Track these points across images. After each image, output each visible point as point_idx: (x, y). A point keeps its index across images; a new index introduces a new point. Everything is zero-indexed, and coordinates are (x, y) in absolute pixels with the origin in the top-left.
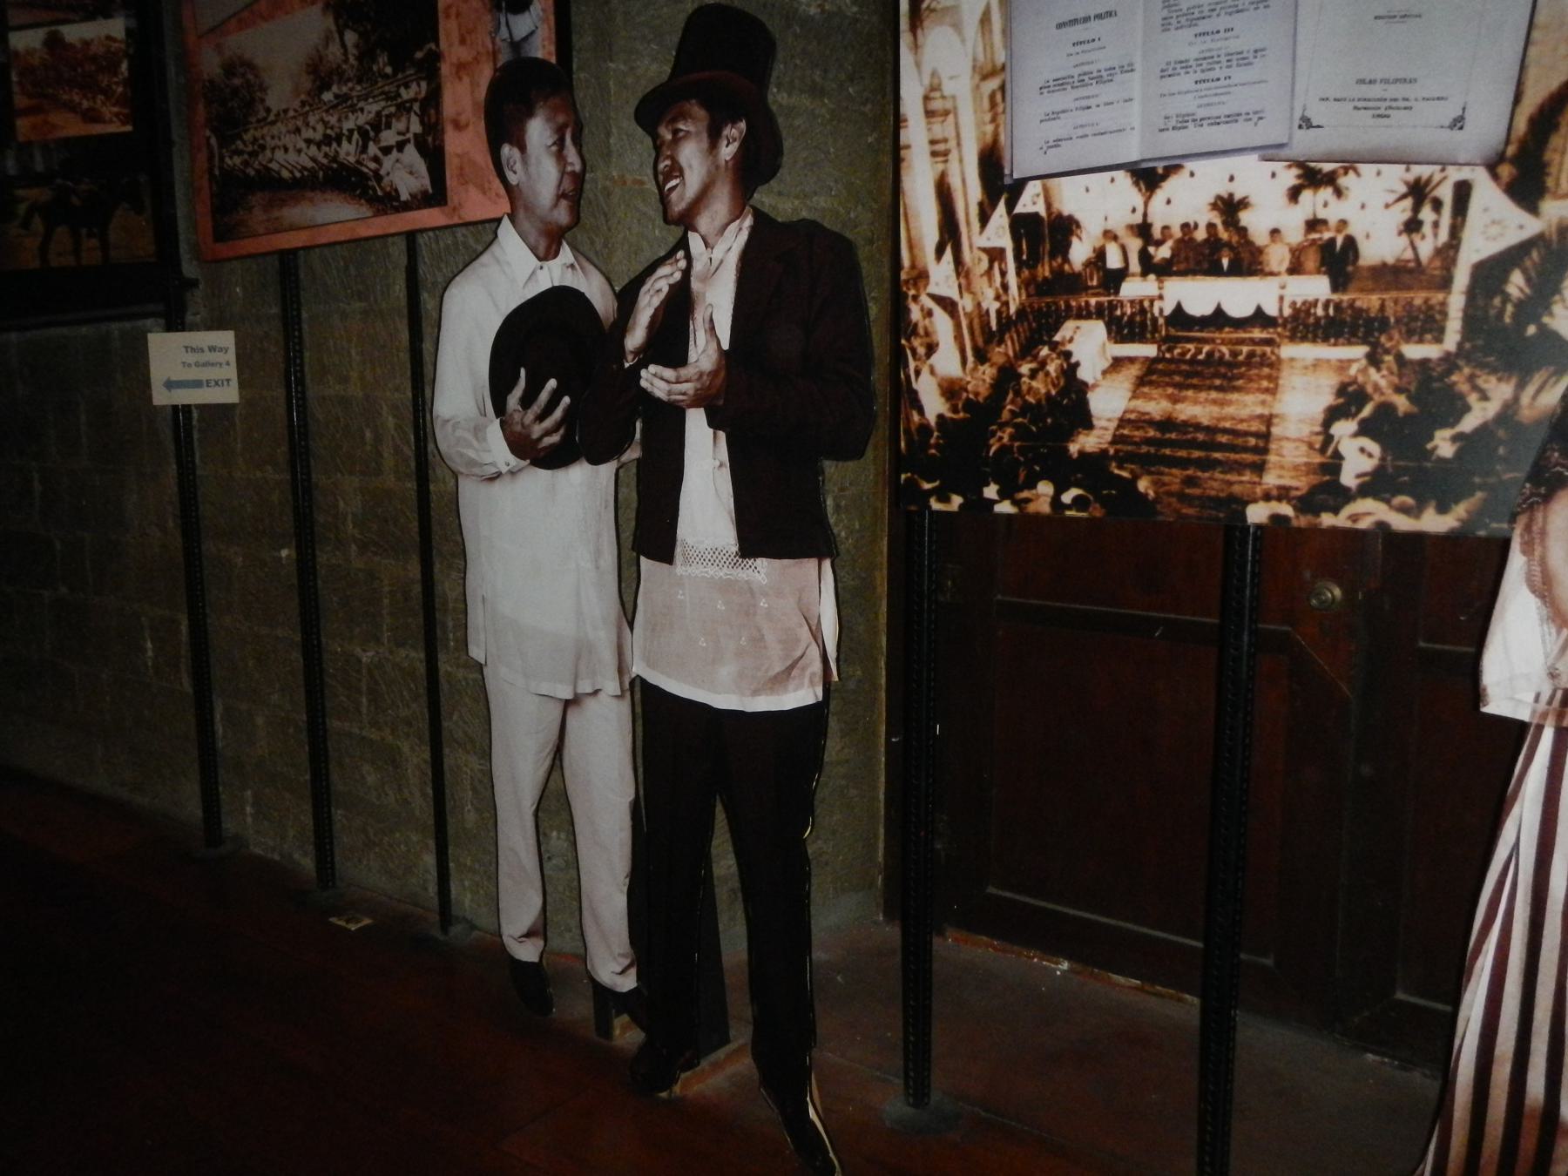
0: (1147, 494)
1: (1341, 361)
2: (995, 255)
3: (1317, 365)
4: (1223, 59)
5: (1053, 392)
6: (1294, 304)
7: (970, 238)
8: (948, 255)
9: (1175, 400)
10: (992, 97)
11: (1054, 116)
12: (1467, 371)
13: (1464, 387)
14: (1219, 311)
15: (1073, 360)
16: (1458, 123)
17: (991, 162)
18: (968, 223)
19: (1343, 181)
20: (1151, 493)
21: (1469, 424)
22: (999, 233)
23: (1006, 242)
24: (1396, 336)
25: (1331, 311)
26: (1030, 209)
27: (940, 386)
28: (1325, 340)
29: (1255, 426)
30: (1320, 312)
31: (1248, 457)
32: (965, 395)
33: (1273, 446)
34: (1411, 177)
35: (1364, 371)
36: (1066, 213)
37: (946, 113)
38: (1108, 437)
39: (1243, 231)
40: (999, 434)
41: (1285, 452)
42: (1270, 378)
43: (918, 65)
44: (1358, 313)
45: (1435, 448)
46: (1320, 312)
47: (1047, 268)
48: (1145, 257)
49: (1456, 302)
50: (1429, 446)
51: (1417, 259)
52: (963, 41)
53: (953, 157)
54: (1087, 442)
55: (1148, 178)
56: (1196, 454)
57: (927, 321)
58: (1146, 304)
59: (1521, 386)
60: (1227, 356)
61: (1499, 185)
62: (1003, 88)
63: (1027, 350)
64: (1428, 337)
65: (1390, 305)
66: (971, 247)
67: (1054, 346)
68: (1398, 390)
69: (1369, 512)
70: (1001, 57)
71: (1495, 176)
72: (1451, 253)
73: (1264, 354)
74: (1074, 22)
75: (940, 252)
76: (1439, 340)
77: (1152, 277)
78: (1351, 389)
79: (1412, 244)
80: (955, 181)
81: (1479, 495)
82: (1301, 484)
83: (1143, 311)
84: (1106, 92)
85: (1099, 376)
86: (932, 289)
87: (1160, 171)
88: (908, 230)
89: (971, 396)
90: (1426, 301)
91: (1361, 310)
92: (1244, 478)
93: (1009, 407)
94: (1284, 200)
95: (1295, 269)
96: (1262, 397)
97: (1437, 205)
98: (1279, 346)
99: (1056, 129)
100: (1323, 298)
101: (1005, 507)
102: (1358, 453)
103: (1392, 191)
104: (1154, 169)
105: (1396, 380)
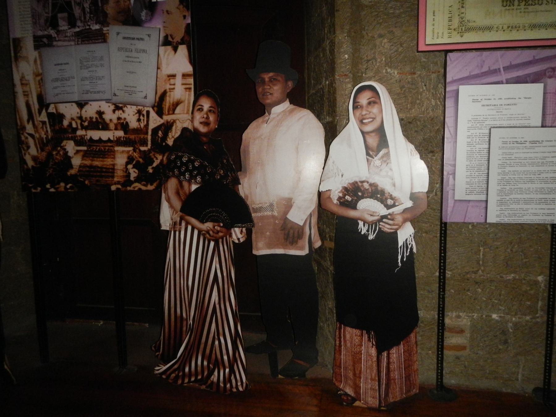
0: (88, 185)
1: (128, 151)
2: (44, 123)
3: (123, 152)
4: (95, 78)
5: (62, 159)
7: (36, 119)
8: (31, 122)
9: (92, 161)
10: (39, 81)
11: (55, 88)
12: (153, 153)
13: (153, 157)
14: (100, 139)
15: (67, 150)
16: (146, 97)
17: (41, 98)
18: (36, 114)
19: (125, 109)
20: (89, 184)
21: (155, 165)
22: (44, 117)
23: (46, 119)
24: (138, 145)
26: (52, 111)
27: (31, 158)
29: (111, 167)
30: (122, 139)
31: (110, 174)
32: (39, 160)
33: (115, 171)
34: (137, 109)
35: (133, 153)
36: (61, 113)
37: (27, 84)
38: (77, 170)
39: (104, 119)
40: (49, 170)
41: (118, 173)
42: (113, 155)
43: (18, 71)
44: (130, 139)
45: (149, 170)
46: (122, 139)
47: (57, 127)
48: (82, 125)
49: (149, 137)
50: (148, 170)
52: (30, 65)
53: (30, 96)
54: (72, 172)
55: (81, 105)
56: (98, 174)
57: (26, 140)
58: (83, 137)
59: (163, 156)
60: (103, 150)
62: (42, 79)
63: (54, 148)
64: (145, 145)
65: (136, 138)
66: (37, 121)
67: (61, 147)
68: (140, 157)
69: (137, 186)
70: (40, 71)
71: (154, 110)
72: (147, 127)
73: (111, 149)
74: (58, 64)
75: (28, 122)
76: (147, 146)
77: (84, 130)
78: (131, 157)
79: (139, 124)
80: (31, 103)
81: (158, 181)
82: (122, 180)
83: (82, 138)
84: (68, 83)
85: (73, 155)
86: (27, 131)
87: (83, 104)
88: (19, 114)
89: (41, 160)
90: (144, 137)
92: (110, 179)
93: (51, 163)
94: (112, 113)
95: (116, 129)
96: (112, 159)
97: (143, 116)
99: (56, 91)
100: (122, 136)
101: (52, 190)
102: (133, 173)
103: (134, 112)
104: (82, 103)
105: (139, 155)
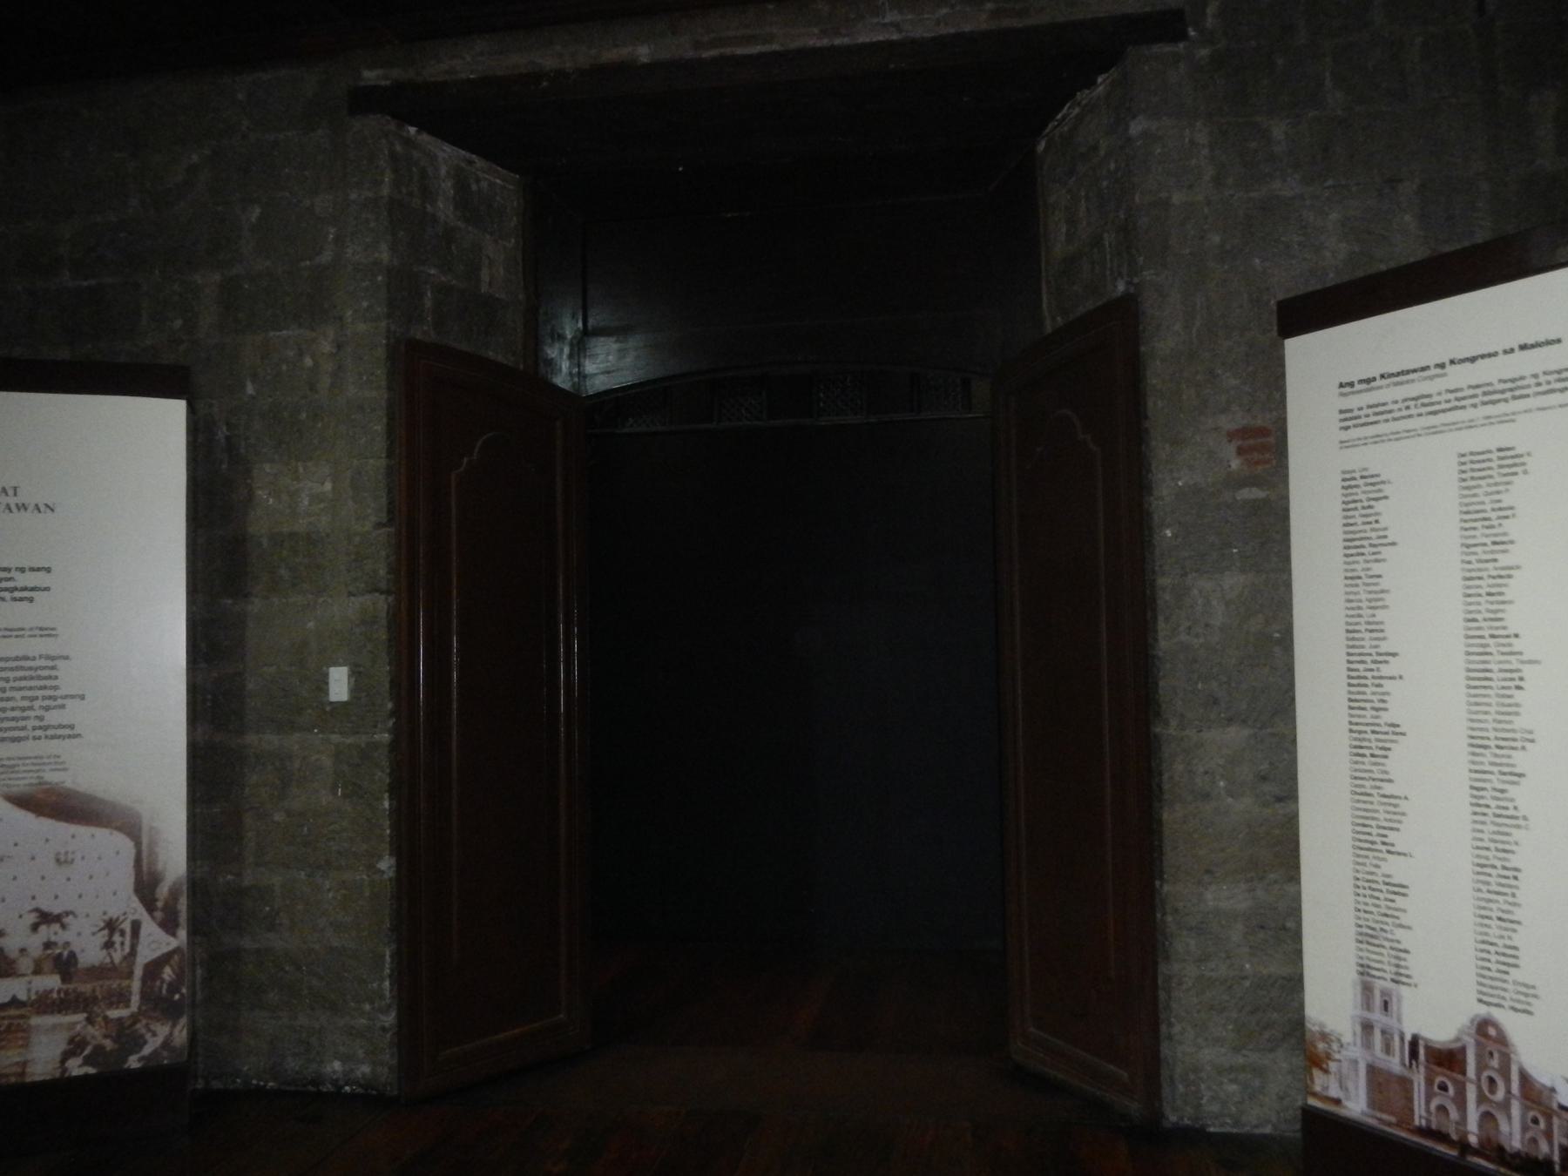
3: (55, 1027)
6: (37, 993)
12: (144, 1022)
13: (143, 1031)
21: (147, 1050)
24: (103, 1007)
25: (62, 995)
28: (59, 1012)
30: (55, 995)
35: (85, 1027)
46: (55, 995)
49: (136, 985)
51: (112, 962)
59: (174, 1026)
61: (156, 922)
65: (98, 989)
68: (106, 1036)
71: (153, 918)
73: (19, 1024)
76: (128, 1006)
78: (77, 1039)
90: (119, 985)
91: (82, 993)
95: (38, 971)
97: (123, 933)
98: (29, 1018)
103: (96, 926)
105: (104, 1030)
